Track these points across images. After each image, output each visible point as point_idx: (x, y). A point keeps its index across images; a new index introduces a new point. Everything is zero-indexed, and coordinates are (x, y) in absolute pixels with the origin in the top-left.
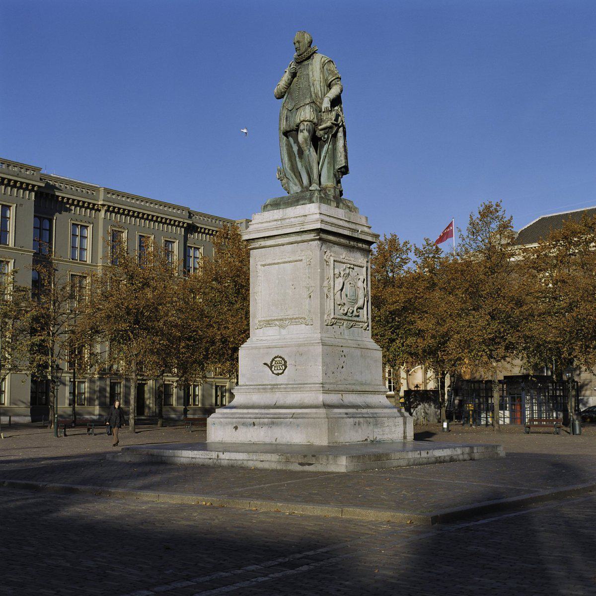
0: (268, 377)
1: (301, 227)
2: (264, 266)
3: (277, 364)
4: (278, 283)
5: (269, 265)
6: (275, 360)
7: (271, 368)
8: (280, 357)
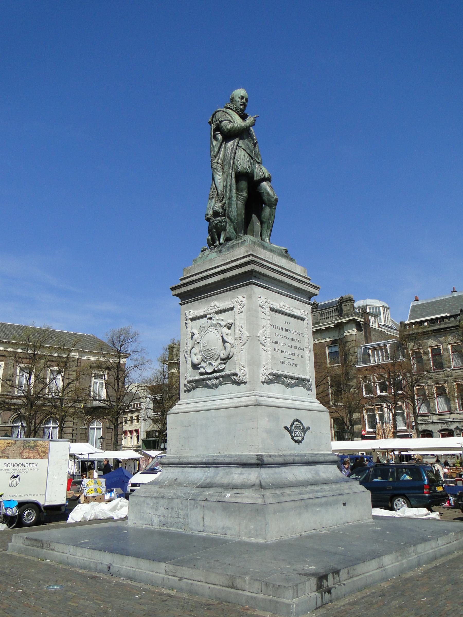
6: (295, 423)
7: (290, 432)
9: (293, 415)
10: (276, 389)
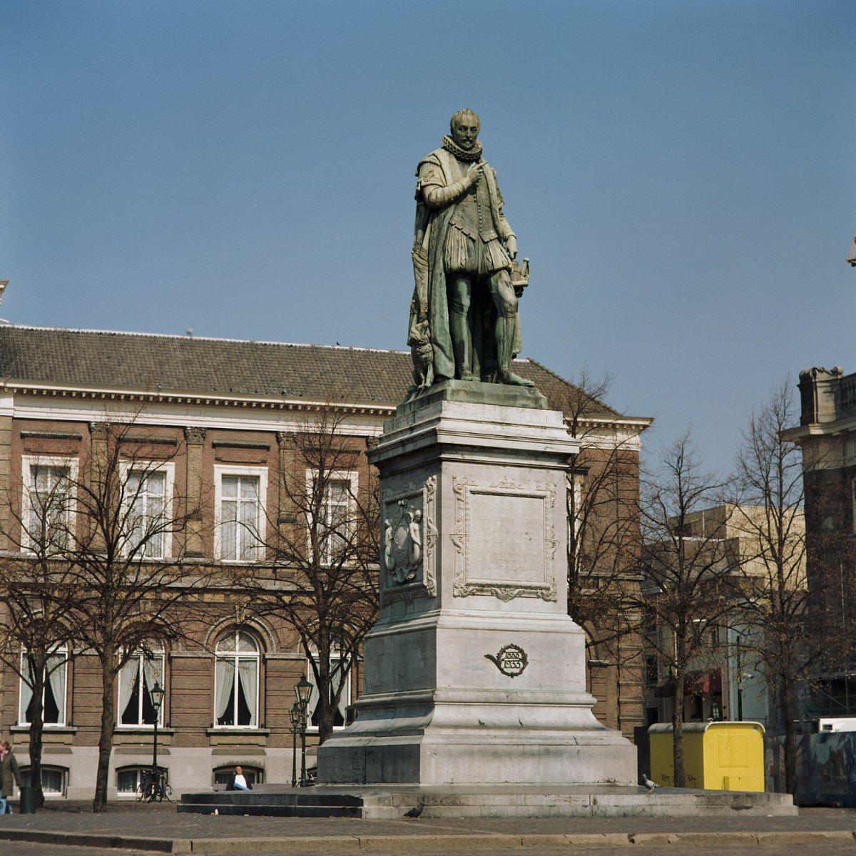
0: (494, 679)
1: (548, 445)
2: (473, 493)
3: (511, 658)
4: (501, 526)
5: (484, 493)
6: (507, 651)
7: (498, 663)
8: (516, 647)
9: (507, 639)
10: (484, 603)
